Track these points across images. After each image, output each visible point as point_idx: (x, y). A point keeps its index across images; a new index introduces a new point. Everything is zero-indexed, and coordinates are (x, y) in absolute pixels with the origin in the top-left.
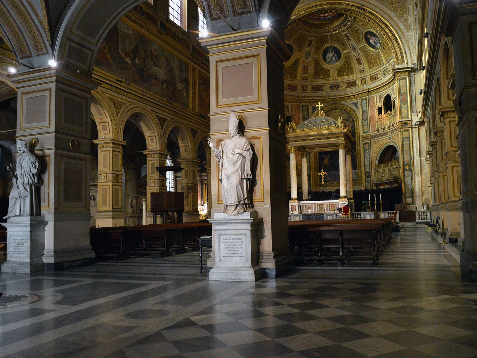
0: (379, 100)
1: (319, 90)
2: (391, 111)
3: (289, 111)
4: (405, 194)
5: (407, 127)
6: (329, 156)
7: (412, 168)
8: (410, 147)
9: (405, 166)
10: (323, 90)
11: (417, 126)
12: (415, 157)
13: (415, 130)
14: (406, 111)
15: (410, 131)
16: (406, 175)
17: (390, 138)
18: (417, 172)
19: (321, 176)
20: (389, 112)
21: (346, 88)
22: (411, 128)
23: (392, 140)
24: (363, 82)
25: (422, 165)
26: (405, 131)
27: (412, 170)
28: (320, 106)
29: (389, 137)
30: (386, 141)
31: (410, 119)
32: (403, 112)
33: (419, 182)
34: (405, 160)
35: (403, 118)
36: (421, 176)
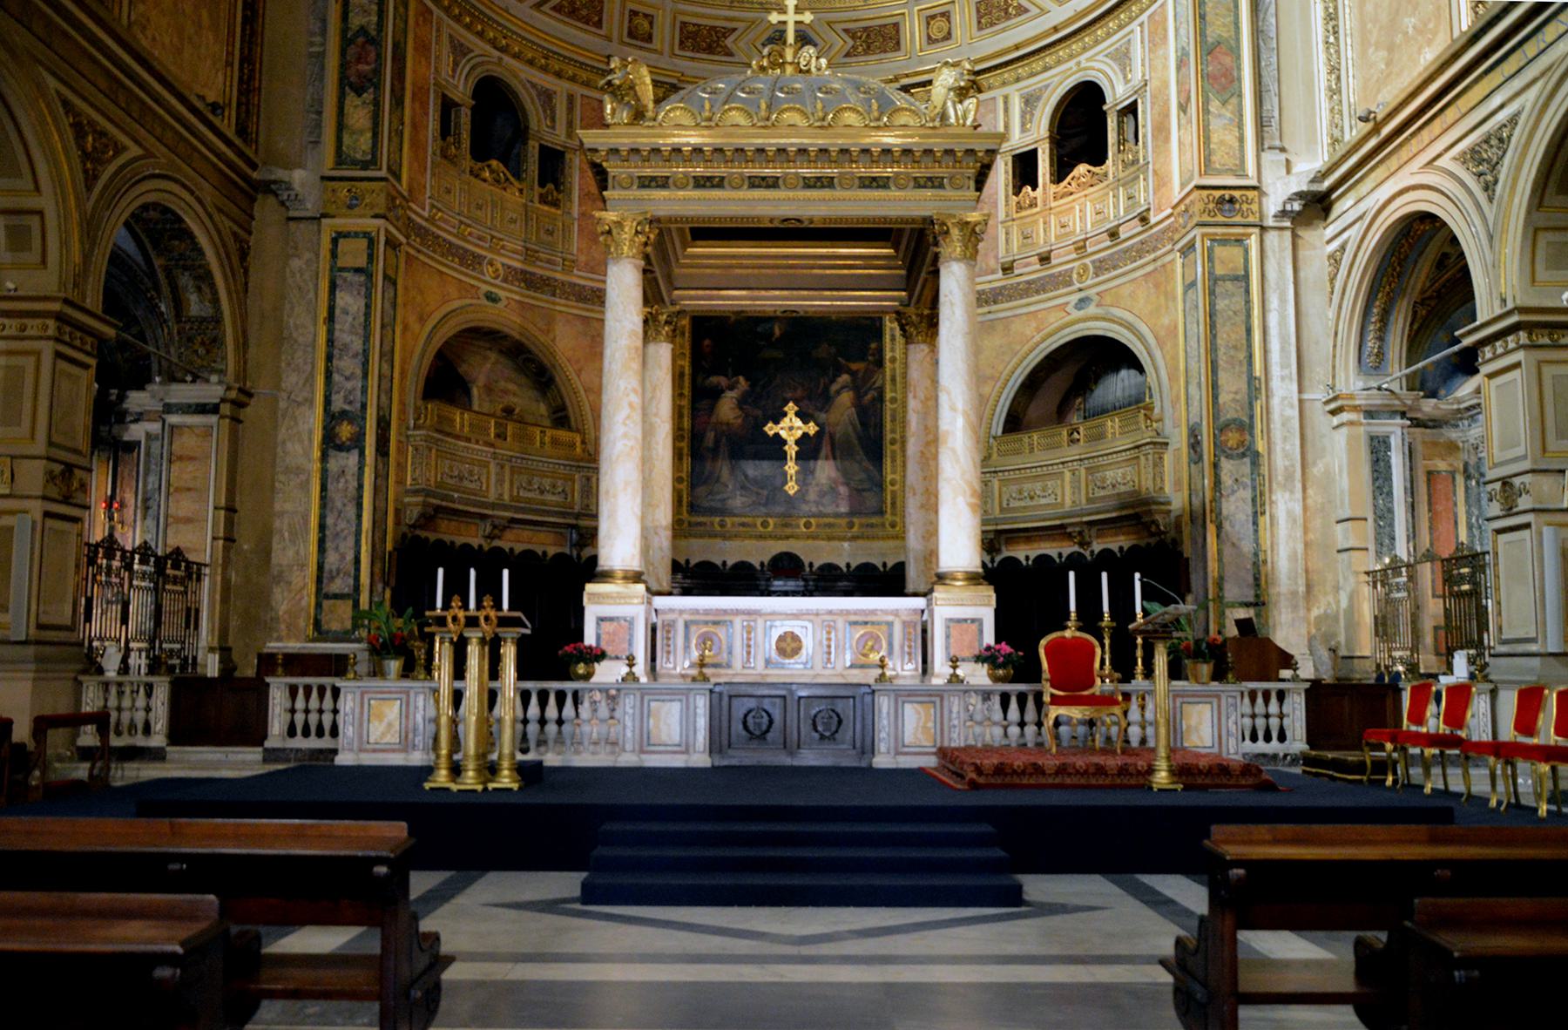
0: (1023, 116)
1: (710, 49)
2: (1098, 158)
3: (553, 120)
4: (1220, 584)
5: (1238, 219)
6: (743, 383)
7: (1261, 446)
8: (1249, 331)
9: (1221, 429)
10: (730, 54)
11: (1288, 224)
12: (1275, 383)
13: (1278, 243)
14: (1231, 139)
15: (1253, 242)
16: (1227, 480)
17: (1083, 303)
18: (1286, 468)
19: (779, 441)
20: (1082, 168)
21: (848, 55)
22: (1257, 230)
23: (1099, 311)
24: (936, 35)
25: (1308, 432)
26: (1224, 241)
27: (1257, 454)
28: (791, 18)
29: (1075, 298)
30: (1055, 320)
31: (1254, 182)
32: (1215, 138)
33: (1295, 521)
34: (1224, 398)
35: (1219, 173)
36: (1304, 489)
